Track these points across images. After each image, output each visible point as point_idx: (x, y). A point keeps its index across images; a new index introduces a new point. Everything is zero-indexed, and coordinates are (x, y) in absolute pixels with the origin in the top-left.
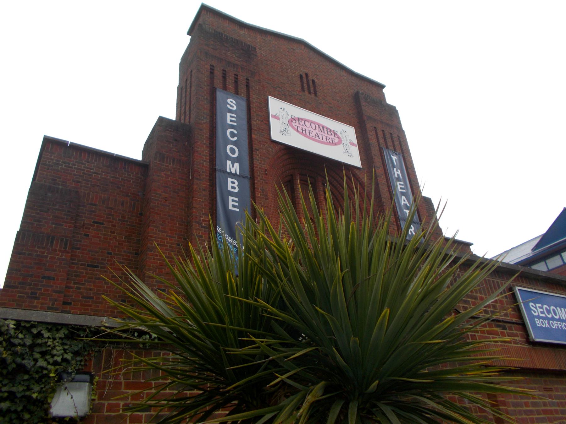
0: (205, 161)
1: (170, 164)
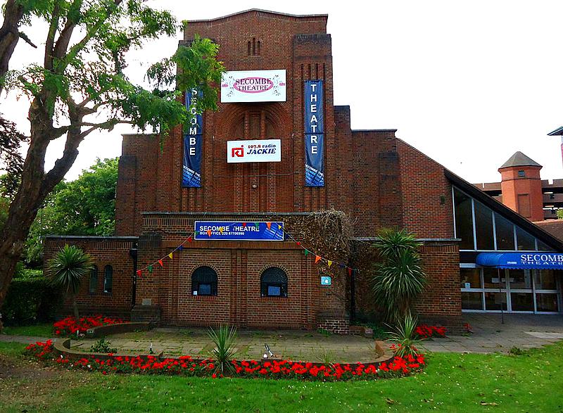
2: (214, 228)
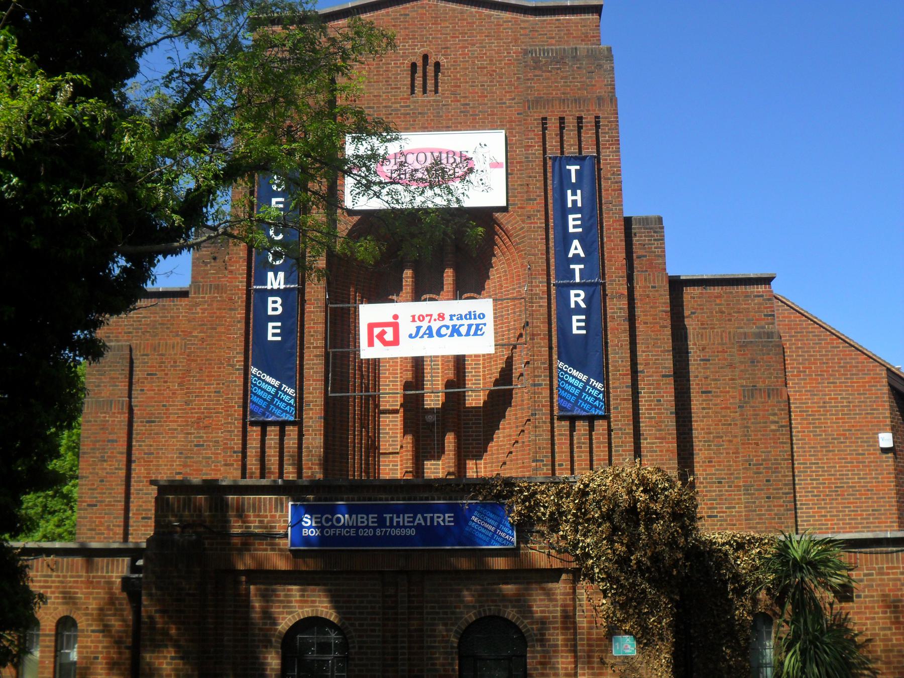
0: (241, 282)
1: (206, 294)
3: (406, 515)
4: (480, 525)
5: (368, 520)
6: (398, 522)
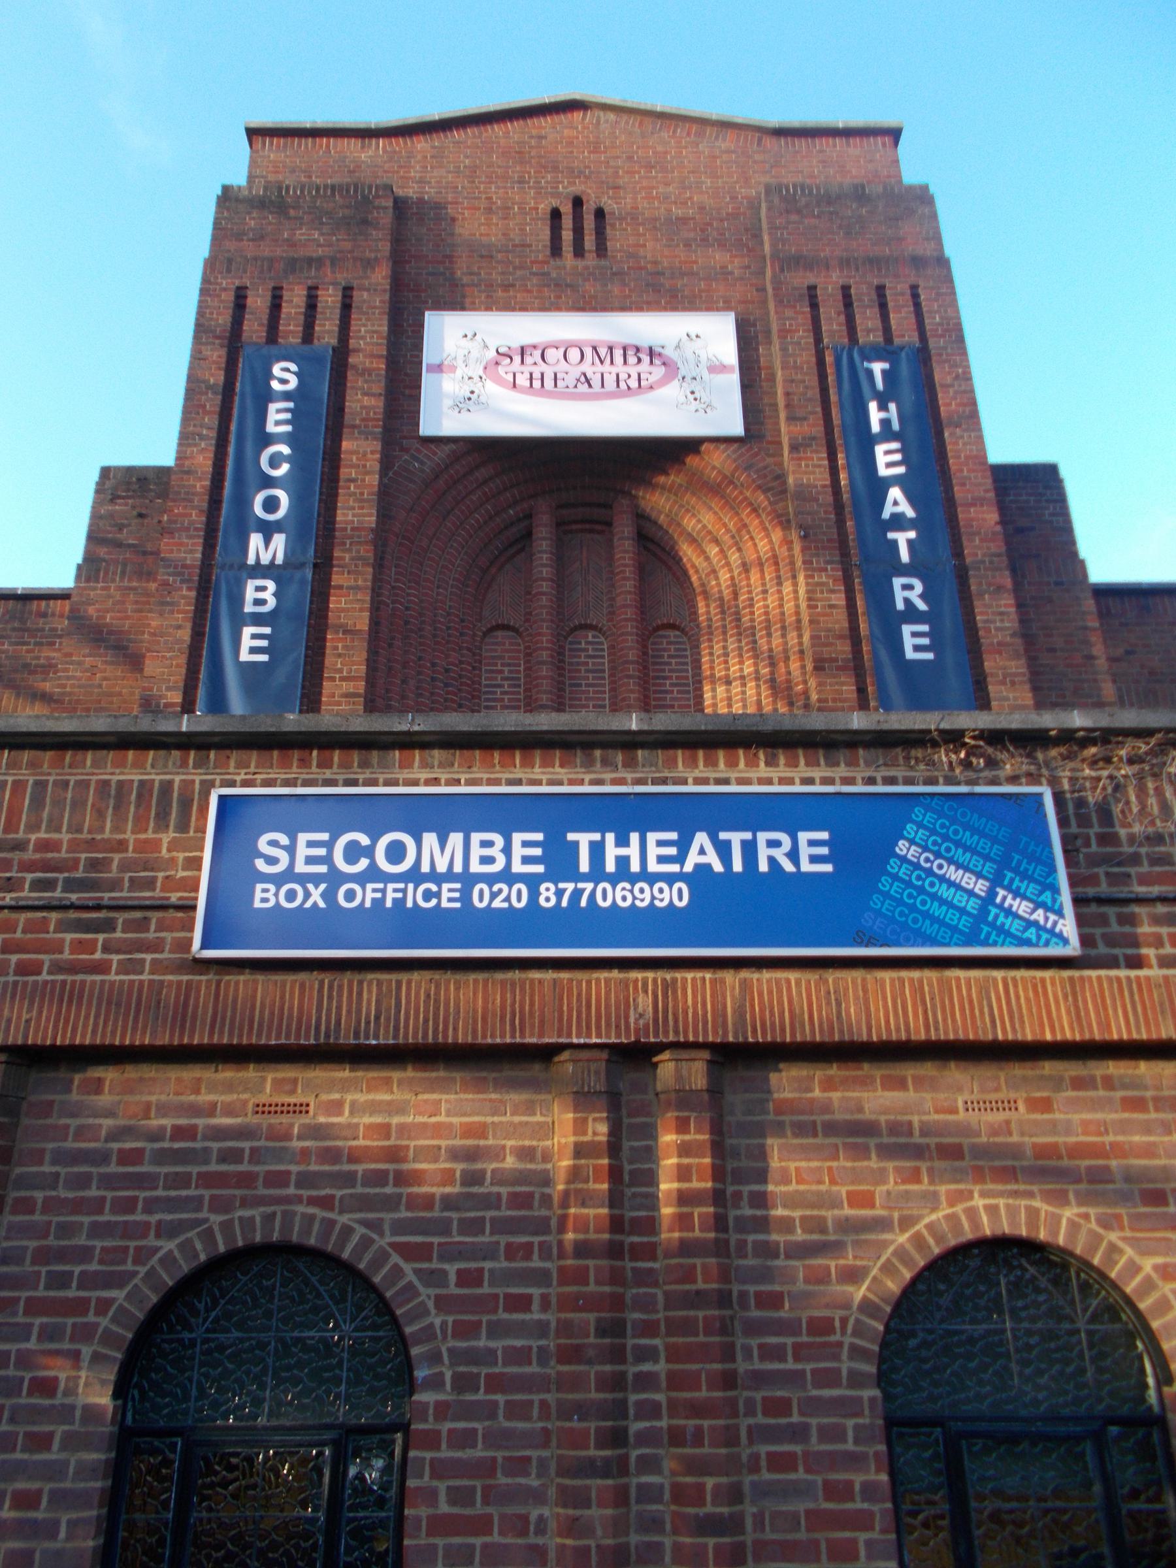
0: (191, 551)
1: (113, 581)
2: (396, 852)
3: (652, 837)
4: (929, 872)
5: (507, 850)
6: (623, 862)
